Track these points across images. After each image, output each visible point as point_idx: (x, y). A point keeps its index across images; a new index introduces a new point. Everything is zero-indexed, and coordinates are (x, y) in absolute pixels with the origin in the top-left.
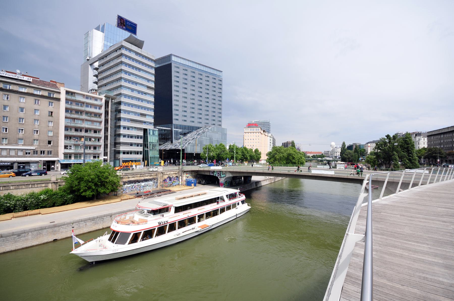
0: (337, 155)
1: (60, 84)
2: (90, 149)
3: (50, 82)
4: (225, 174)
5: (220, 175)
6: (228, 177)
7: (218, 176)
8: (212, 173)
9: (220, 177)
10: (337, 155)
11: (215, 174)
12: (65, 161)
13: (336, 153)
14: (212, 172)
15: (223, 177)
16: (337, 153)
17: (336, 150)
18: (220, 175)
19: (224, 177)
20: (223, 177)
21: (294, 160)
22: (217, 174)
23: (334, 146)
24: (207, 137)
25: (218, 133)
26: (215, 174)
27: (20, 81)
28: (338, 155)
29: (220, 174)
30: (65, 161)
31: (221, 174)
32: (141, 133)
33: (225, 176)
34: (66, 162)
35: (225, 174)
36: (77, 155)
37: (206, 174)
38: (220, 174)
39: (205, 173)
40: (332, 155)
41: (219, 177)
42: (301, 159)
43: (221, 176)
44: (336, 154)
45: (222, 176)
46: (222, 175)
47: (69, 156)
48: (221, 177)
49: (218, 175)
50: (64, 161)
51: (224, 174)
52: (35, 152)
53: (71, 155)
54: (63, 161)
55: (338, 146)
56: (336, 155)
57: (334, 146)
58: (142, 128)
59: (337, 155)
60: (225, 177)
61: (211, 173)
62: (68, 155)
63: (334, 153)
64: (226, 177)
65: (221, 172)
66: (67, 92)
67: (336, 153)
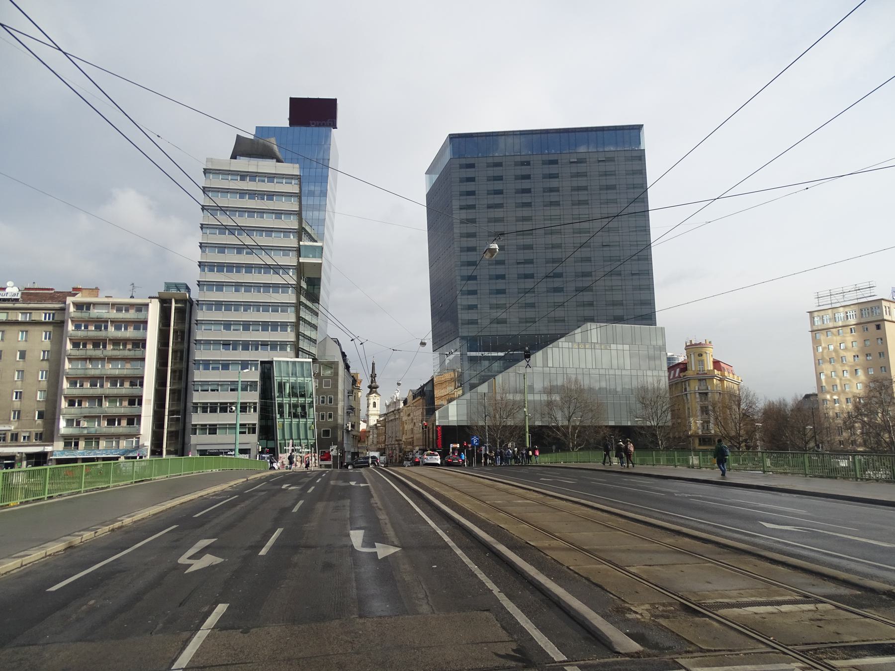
1: (91, 290)
2: (119, 424)
3: (71, 290)
12: (66, 453)
24: (550, 365)
25: (613, 346)
27: (3, 301)
30: (64, 454)
32: (254, 375)
34: (67, 456)
36: (92, 439)
47: (74, 442)
50: (62, 453)
52: (15, 437)
53: (78, 439)
54: (61, 453)
58: (258, 361)
62: (72, 439)
66: (79, 306)
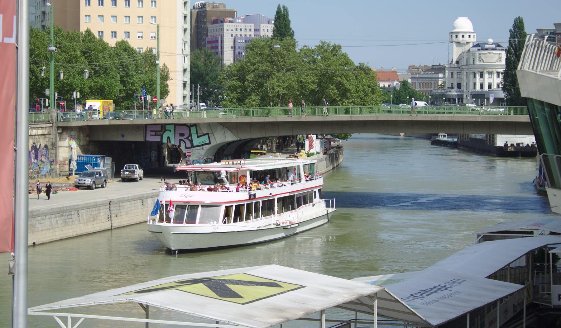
0: (482, 86)
4: (208, 134)
5: (187, 141)
6: (218, 142)
7: (182, 144)
8: (156, 135)
9: (189, 145)
10: (482, 86)
11: (169, 138)
13: (478, 76)
14: (156, 132)
15: (203, 145)
16: (486, 76)
17: (477, 62)
18: (187, 138)
19: (206, 144)
20: (203, 145)
21: (348, 98)
22: (178, 135)
23: (466, 36)
26: (169, 138)
28: (490, 87)
29: (190, 135)
31: (194, 136)
33: (208, 142)
35: (208, 134)
37: (130, 138)
38: (186, 136)
39: (123, 136)
40: (459, 86)
41: (183, 147)
42: (374, 96)
43: (191, 142)
44: (478, 80)
45: (196, 141)
46: (198, 137)
48: (192, 146)
49: (180, 140)
51: (204, 135)
55: (491, 41)
56: (478, 87)
57: (467, 38)
59: (486, 88)
60: (210, 143)
61: (149, 133)
63: (472, 76)
64: (213, 143)
65: (193, 130)
67: (478, 76)
